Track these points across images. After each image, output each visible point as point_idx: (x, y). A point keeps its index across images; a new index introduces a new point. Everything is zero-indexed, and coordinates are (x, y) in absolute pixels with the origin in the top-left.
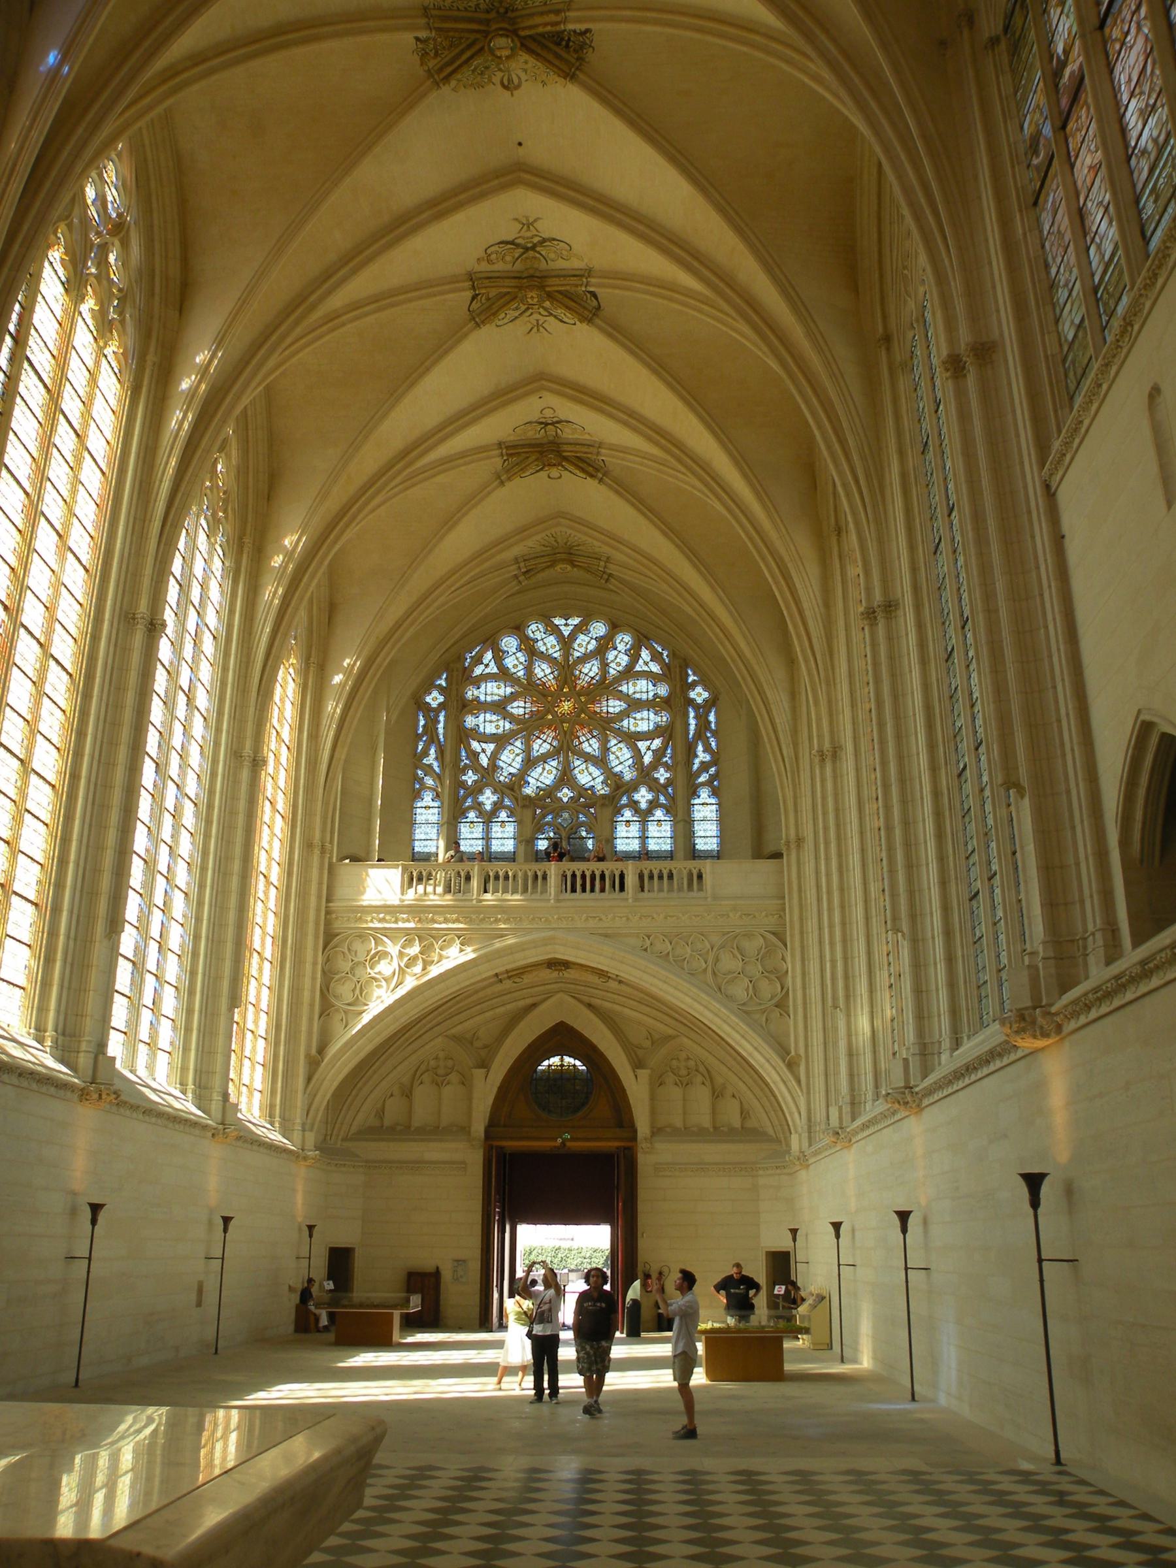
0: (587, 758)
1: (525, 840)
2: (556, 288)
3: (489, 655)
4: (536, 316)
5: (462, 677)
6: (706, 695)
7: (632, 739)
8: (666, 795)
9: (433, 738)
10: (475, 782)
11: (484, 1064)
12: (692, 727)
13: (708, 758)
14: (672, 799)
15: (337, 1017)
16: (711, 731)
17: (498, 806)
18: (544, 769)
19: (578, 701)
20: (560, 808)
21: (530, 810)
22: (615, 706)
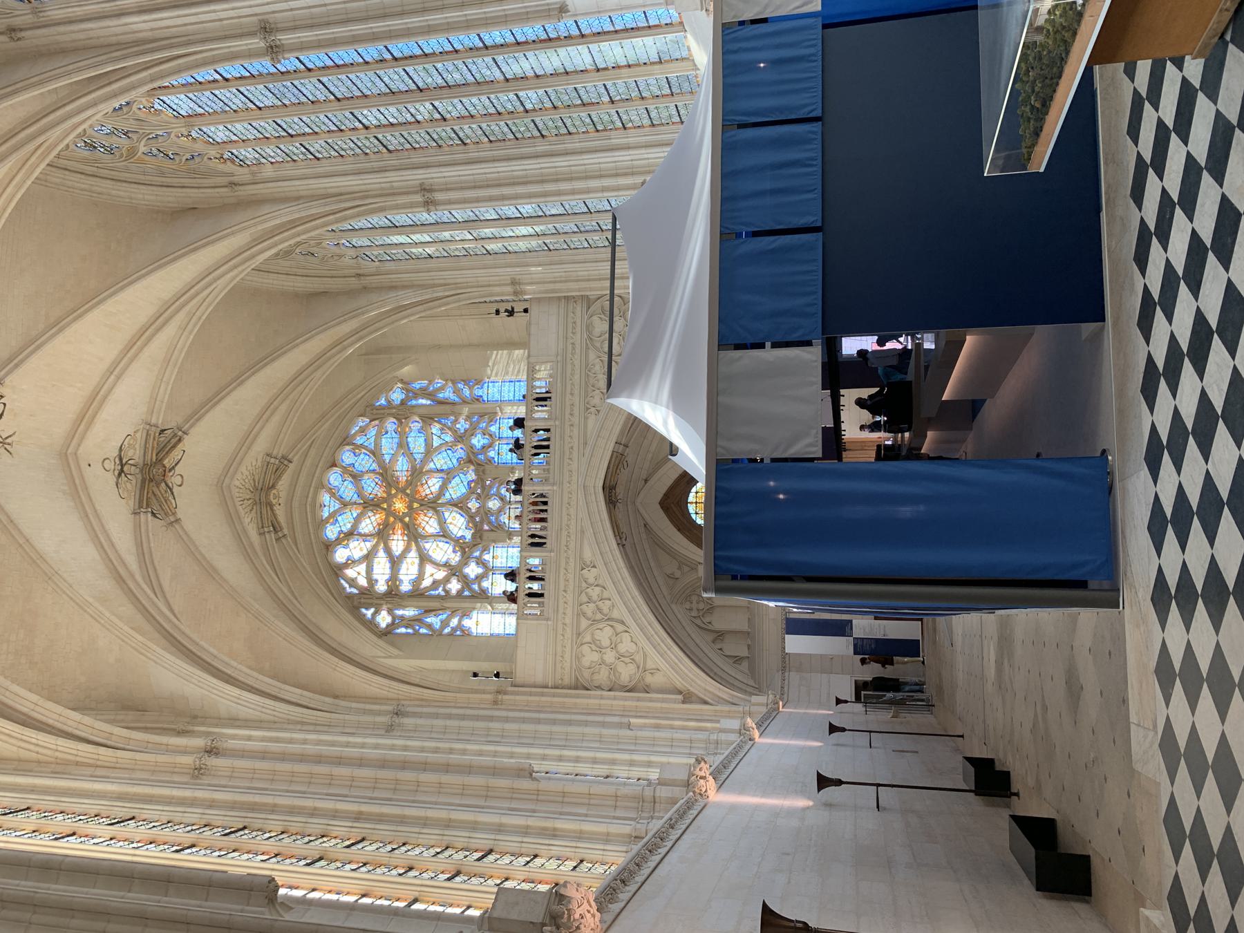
0: (443, 488)
3: (350, 573)
5: (368, 596)
7: (429, 451)
9: (417, 620)
14: (482, 416)
15: (649, 679)
17: (480, 562)
21: (485, 531)
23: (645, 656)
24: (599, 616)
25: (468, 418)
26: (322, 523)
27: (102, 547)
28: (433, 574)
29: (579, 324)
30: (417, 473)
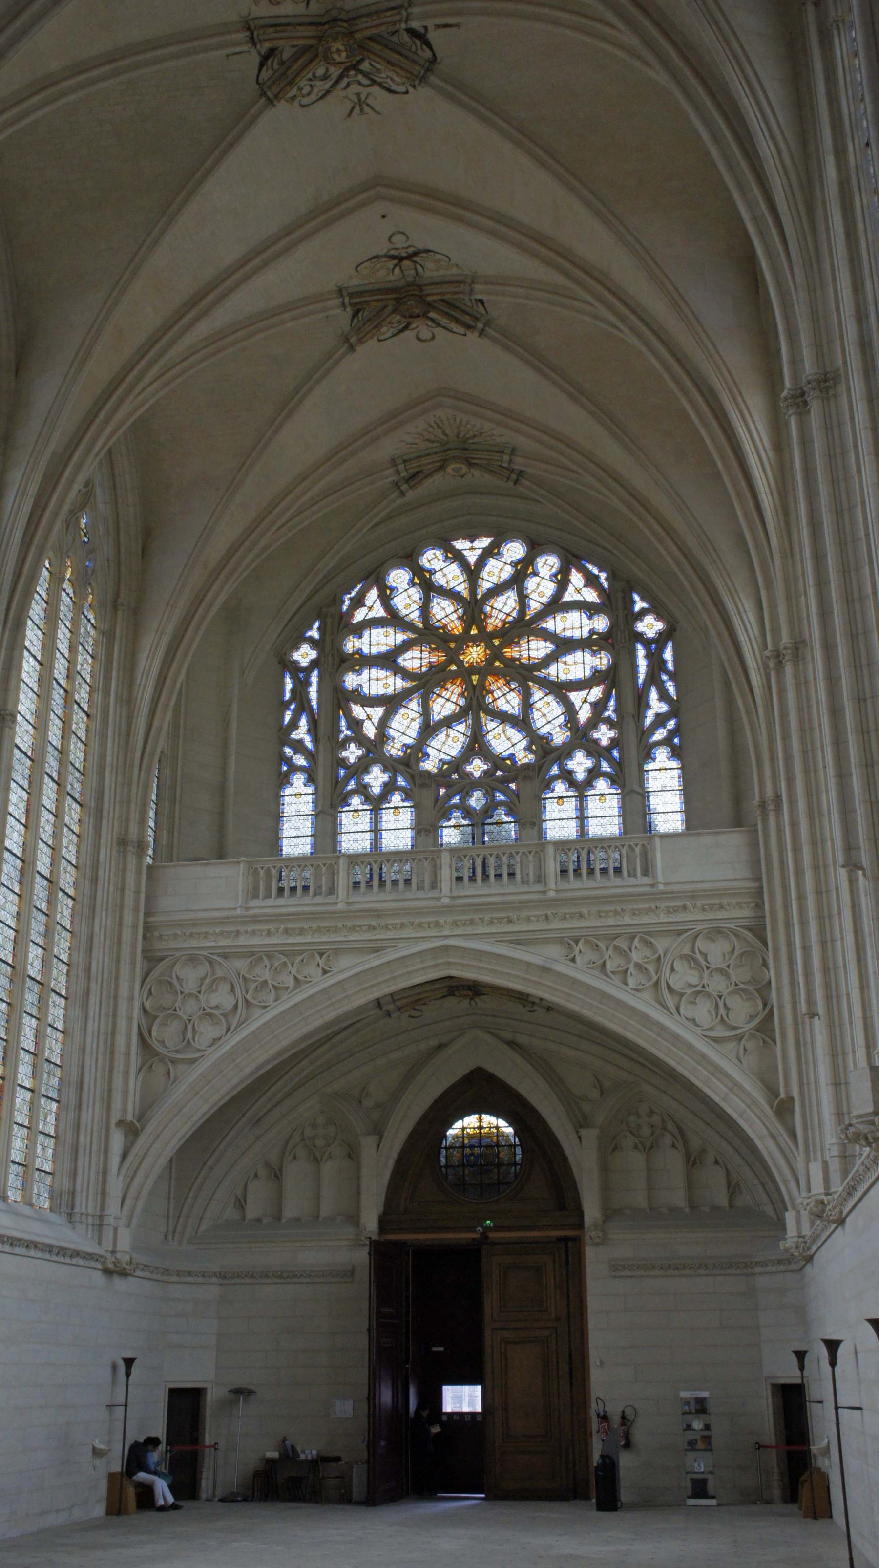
0: (504, 718)
1: (426, 829)
2: (368, 33)
3: (373, 595)
4: (355, 88)
6: (659, 626)
7: (560, 690)
8: (610, 760)
10: (360, 758)
11: (378, 1131)
13: (663, 708)
14: (618, 765)
16: (667, 672)
17: (389, 788)
18: (448, 736)
19: (489, 646)
20: (468, 785)
21: (431, 792)
22: (539, 649)
23: (193, 1061)
26: (445, 545)
27: (243, 265)
28: (370, 718)
29: (720, 915)
30: (524, 675)
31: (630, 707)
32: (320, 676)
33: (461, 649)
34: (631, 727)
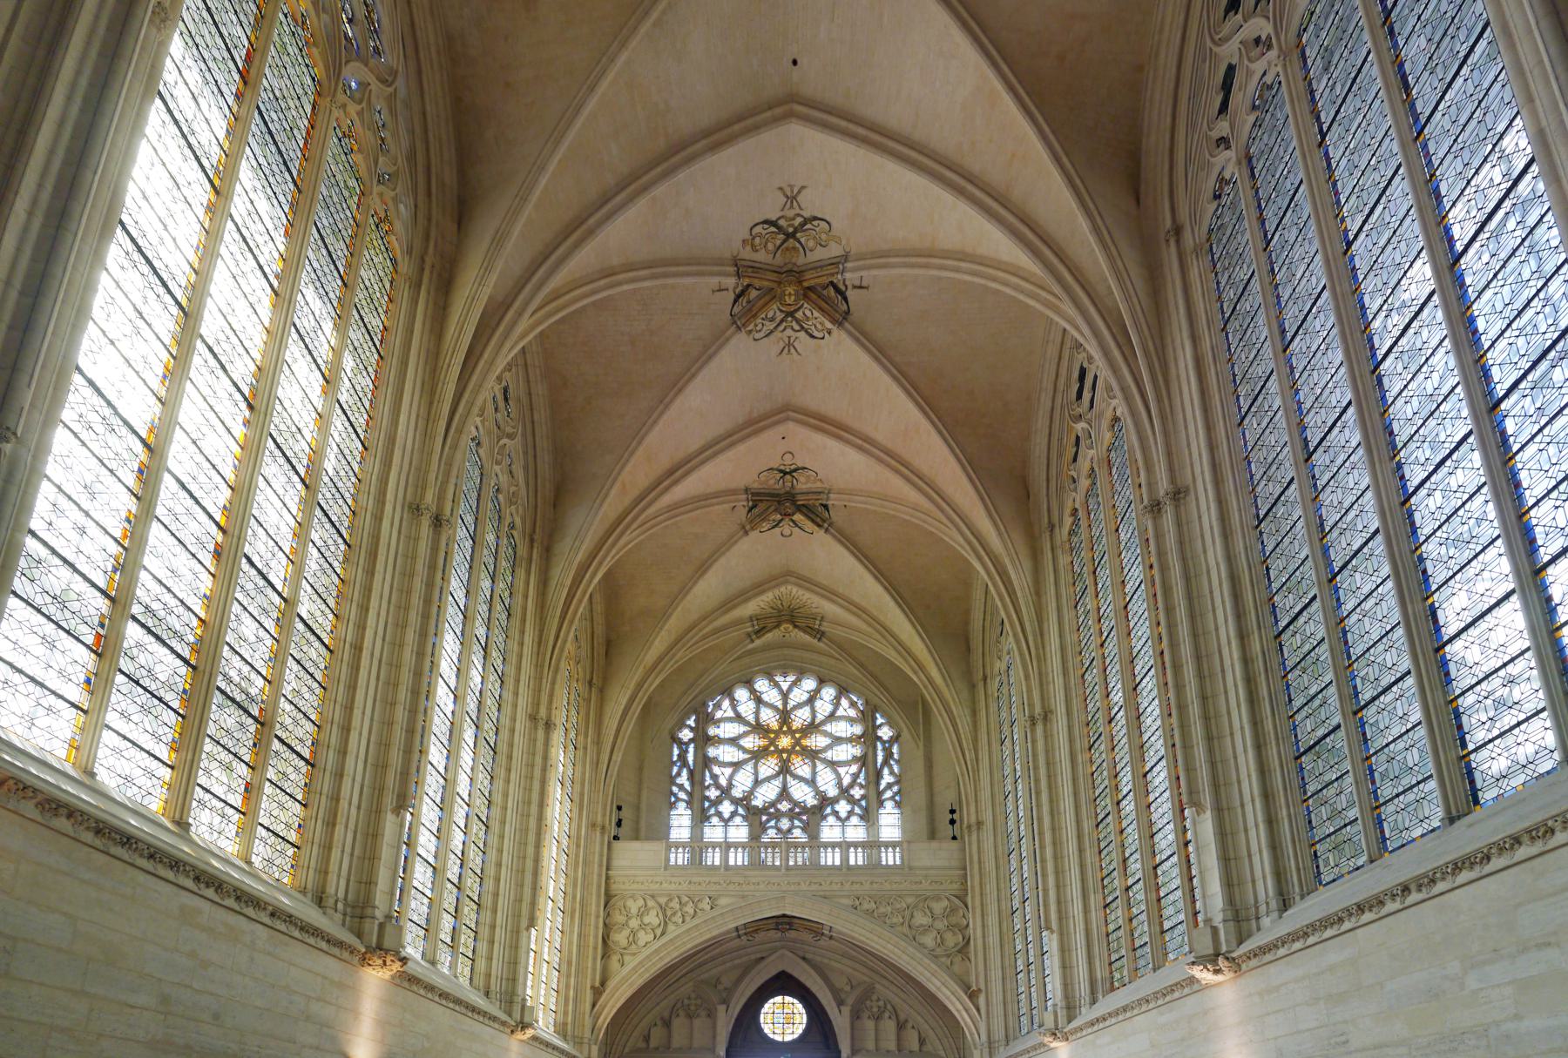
0: (801, 779)
3: (726, 704)
5: (706, 719)
7: (833, 765)
8: (860, 806)
9: (684, 763)
12: (880, 759)
15: (615, 958)
17: (734, 814)
21: (756, 816)
24: (669, 913)
25: (863, 797)
28: (723, 774)
30: (812, 755)
31: (872, 778)
32: (696, 749)
33: (777, 737)
34: (872, 787)
